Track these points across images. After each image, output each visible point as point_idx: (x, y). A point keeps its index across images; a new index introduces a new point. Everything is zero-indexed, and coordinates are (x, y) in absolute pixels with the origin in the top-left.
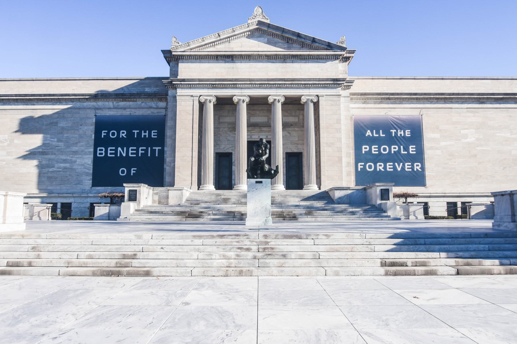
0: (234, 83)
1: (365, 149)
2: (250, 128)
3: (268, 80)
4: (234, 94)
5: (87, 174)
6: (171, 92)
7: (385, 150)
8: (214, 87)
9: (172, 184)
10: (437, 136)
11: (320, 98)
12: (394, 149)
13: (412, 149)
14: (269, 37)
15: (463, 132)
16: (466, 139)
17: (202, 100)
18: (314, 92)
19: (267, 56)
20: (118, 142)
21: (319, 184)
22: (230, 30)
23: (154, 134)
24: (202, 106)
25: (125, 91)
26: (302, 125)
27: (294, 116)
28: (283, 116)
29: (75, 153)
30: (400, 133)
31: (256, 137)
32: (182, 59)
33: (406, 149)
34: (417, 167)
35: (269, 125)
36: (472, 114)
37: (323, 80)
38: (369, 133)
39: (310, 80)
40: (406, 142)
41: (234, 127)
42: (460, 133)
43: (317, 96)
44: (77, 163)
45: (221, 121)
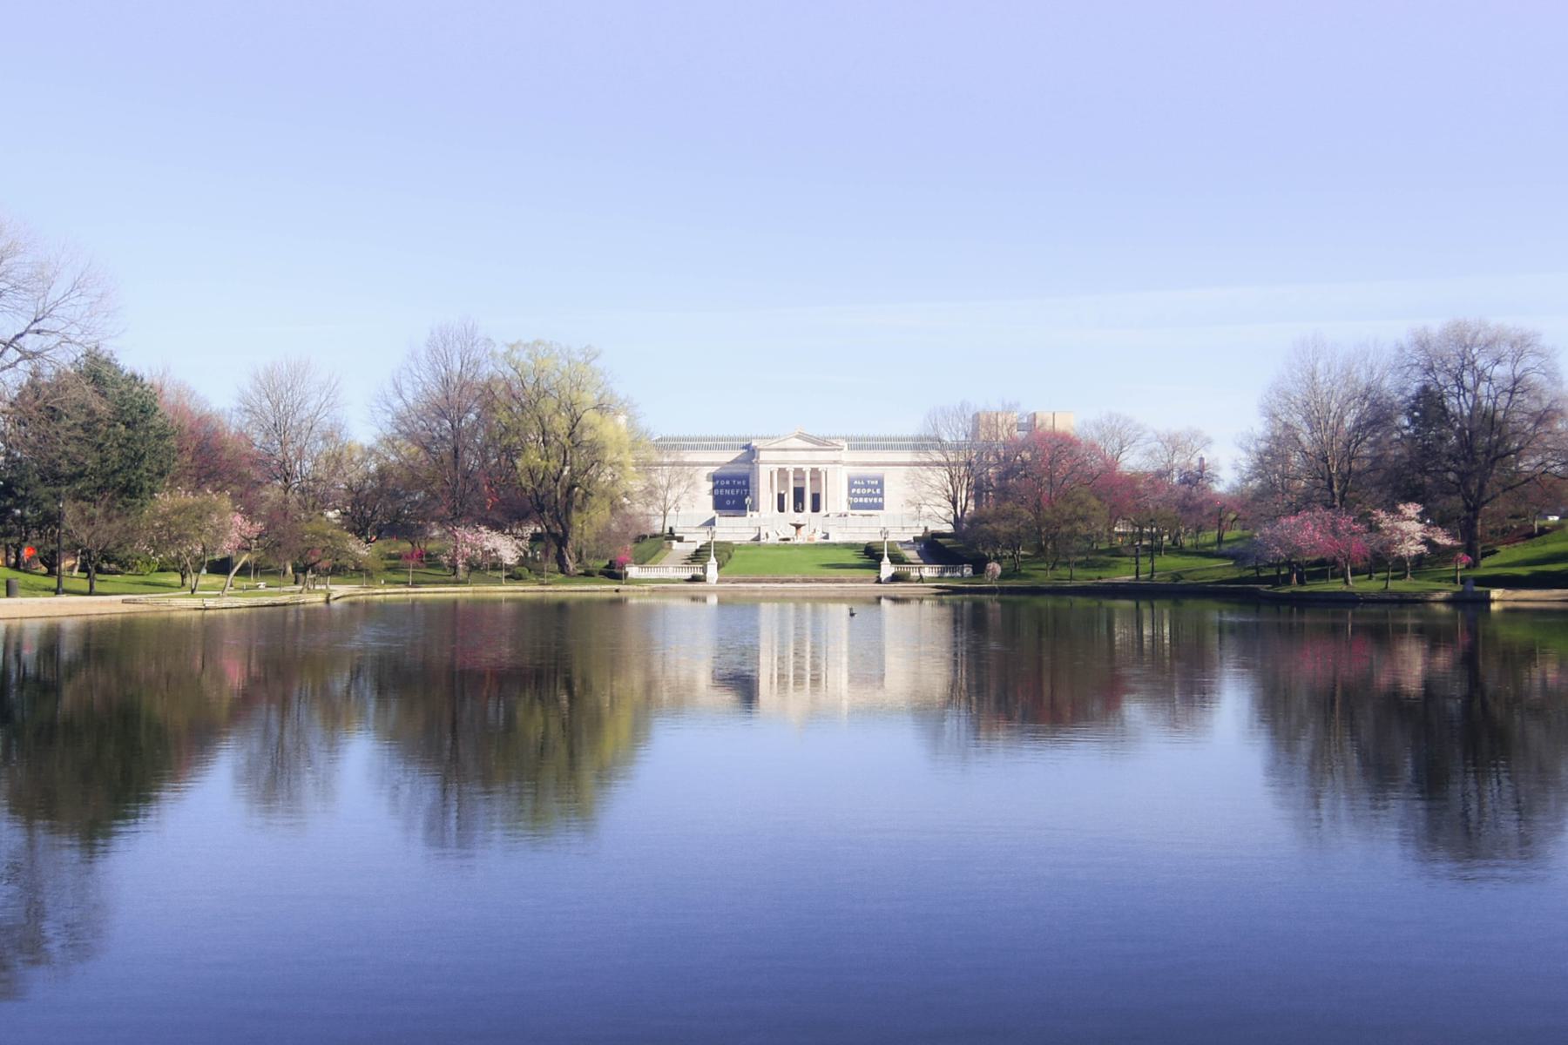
1: (854, 490)
6: (756, 464)
7: (864, 491)
9: (758, 511)
12: (869, 490)
13: (878, 491)
20: (726, 487)
23: (744, 483)
24: (771, 473)
26: (819, 479)
30: (873, 482)
31: (796, 486)
33: (875, 490)
34: (880, 500)
35: (804, 479)
38: (856, 482)
40: (875, 487)
41: (787, 479)
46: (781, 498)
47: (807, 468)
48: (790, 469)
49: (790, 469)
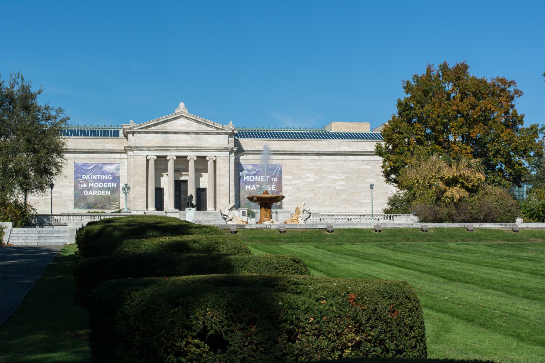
0: (167, 149)
2: (176, 173)
3: (187, 147)
4: (167, 155)
5: (70, 200)
8: (156, 150)
10: (291, 177)
11: (217, 158)
14: (188, 120)
15: (307, 175)
16: (308, 179)
17: (148, 158)
18: (214, 154)
19: (187, 132)
21: (215, 207)
22: (165, 117)
24: (148, 161)
25: (93, 147)
27: (202, 165)
28: (195, 165)
29: (62, 186)
32: (136, 133)
36: (313, 164)
37: (219, 147)
39: (211, 147)
42: (305, 175)
43: (215, 156)
44: (64, 193)
45: (156, 168)
46: (159, 192)
47: (192, 156)
48: (171, 156)
49: (171, 156)
